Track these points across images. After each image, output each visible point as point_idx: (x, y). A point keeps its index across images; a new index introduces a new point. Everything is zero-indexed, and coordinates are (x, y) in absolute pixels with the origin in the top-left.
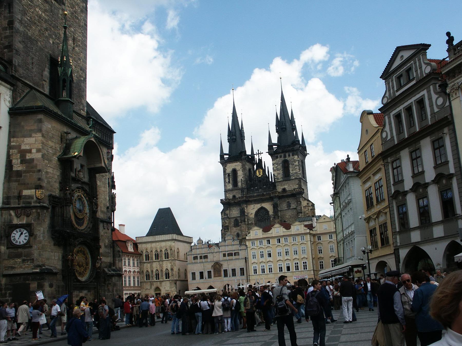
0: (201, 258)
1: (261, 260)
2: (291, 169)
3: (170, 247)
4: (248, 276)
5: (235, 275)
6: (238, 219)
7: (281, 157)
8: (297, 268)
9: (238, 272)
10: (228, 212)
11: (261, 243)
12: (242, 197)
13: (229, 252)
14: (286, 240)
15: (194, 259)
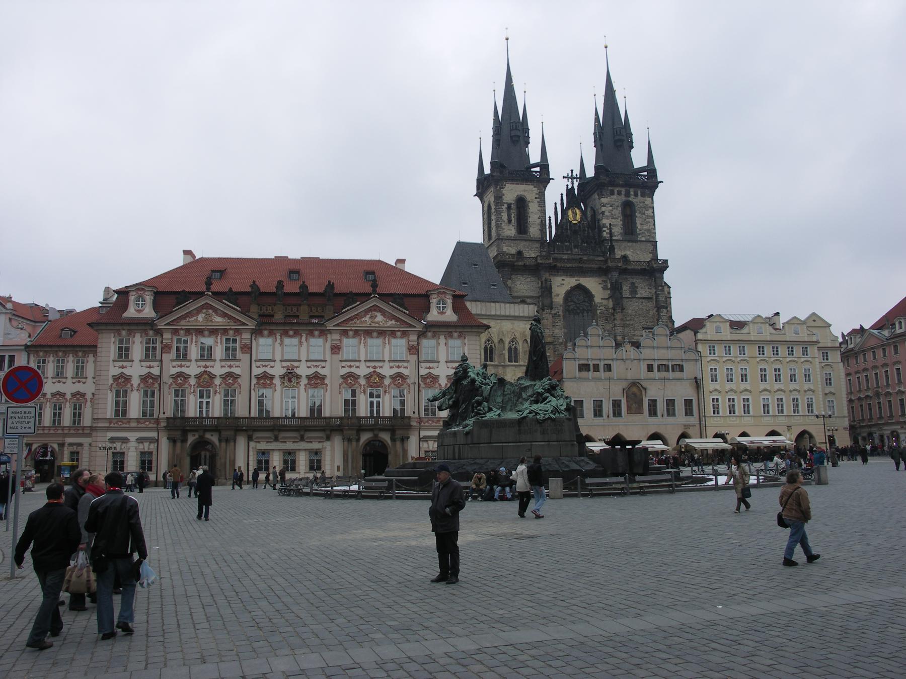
0: (596, 368)
1: (728, 386)
2: (638, 222)
3: (523, 334)
4: (702, 418)
5: (674, 415)
6: (528, 301)
7: (619, 193)
8: (796, 407)
9: (680, 407)
10: (509, 282)
11: (728, 350)
12: (547, 257)
13: (660, 363)
14: (776, 351)
15: (580, 370)
